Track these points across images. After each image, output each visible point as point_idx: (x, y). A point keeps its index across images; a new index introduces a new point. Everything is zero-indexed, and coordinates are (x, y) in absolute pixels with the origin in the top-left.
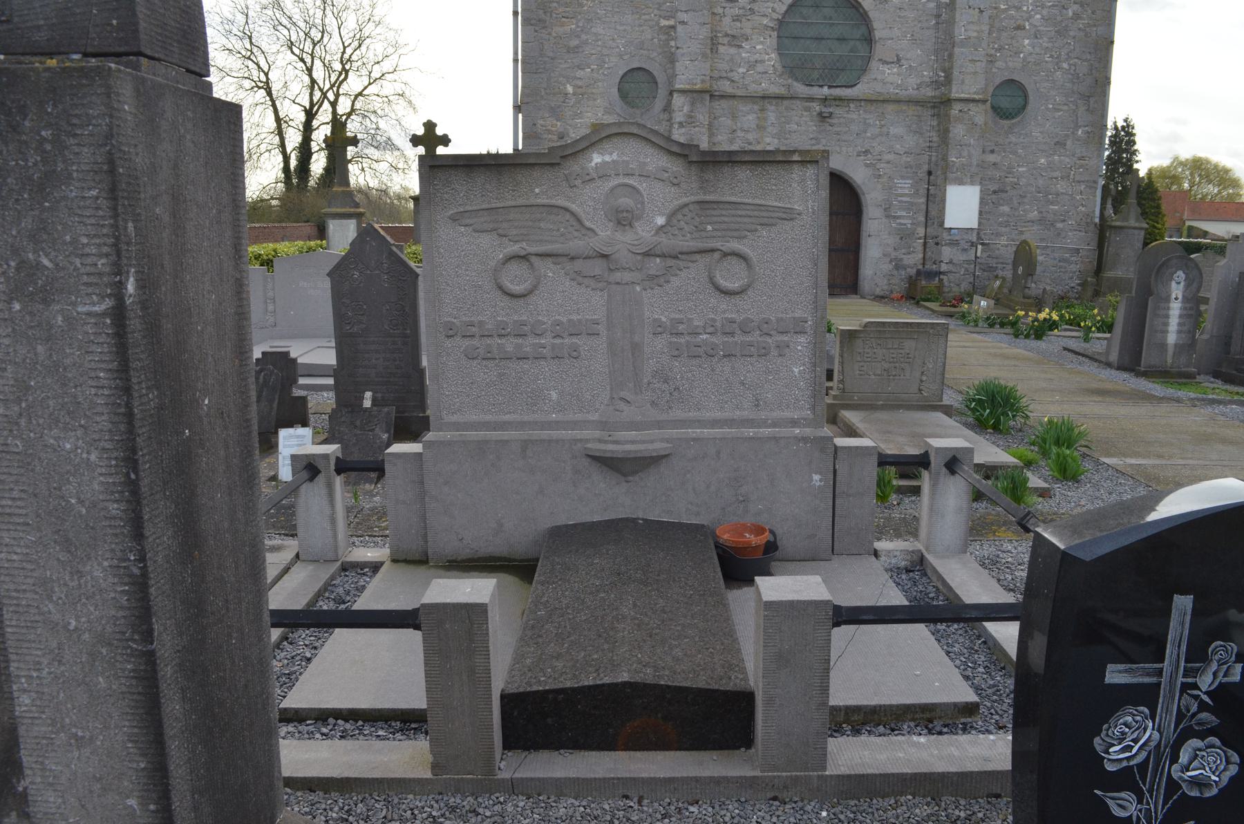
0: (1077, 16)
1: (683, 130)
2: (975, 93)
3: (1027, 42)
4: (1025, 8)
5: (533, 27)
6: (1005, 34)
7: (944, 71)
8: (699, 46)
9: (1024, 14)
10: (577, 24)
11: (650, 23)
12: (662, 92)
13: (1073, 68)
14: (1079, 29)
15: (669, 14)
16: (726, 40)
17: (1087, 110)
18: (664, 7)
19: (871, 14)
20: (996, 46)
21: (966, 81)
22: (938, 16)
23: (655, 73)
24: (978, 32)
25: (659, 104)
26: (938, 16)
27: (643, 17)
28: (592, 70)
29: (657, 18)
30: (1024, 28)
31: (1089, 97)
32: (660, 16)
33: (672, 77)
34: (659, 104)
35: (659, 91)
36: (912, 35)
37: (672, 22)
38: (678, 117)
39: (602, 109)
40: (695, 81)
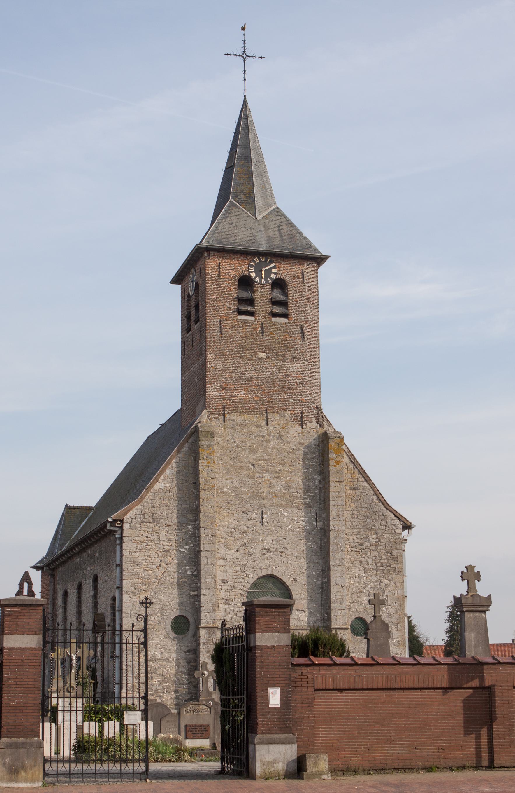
0: (387, 586)
1: (205, 647)
2: (342, 625)
3: (364, 598)
4: (363, 583)
5: (129, 596)
6: (354, 595)
7: (327, 614)
8: (211, 605)
9: (362, 585)
10: (150, 594)
11: (186, 593)
12: (192, 627)
13: (388, 610)
14: (389, 592)
15: (194, 589)
16: (223, 601)
17: (397, 630)
18: (192, 586)
19: (291, 588)
20: (351, 601)
21: (338, 620)
22: (322, 588)
23: (189, 618)
24: (341, 596)
25: (190, 633)
26: (322, 588)
27: (182, 590)
28: (158, 616)
29: (189, 591)
30: (363, 592)
31: (397, 624)
32: (191, 590)
33: (198, 621)
34: (190, 633)
35: (191, 626)
36: (311, 597)
37: (196, 593)
38: (202, 640)
39: (163, 636)
40: (210, 622)
